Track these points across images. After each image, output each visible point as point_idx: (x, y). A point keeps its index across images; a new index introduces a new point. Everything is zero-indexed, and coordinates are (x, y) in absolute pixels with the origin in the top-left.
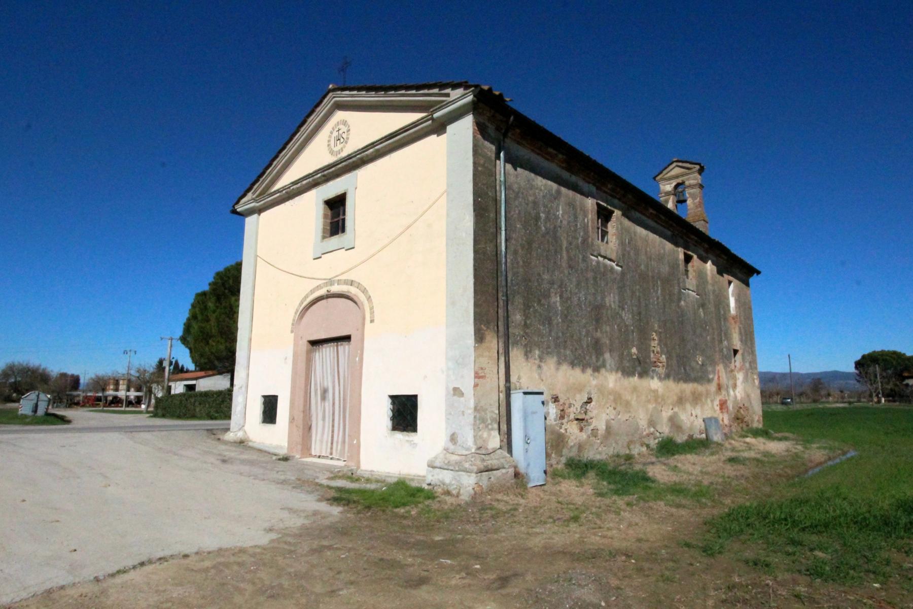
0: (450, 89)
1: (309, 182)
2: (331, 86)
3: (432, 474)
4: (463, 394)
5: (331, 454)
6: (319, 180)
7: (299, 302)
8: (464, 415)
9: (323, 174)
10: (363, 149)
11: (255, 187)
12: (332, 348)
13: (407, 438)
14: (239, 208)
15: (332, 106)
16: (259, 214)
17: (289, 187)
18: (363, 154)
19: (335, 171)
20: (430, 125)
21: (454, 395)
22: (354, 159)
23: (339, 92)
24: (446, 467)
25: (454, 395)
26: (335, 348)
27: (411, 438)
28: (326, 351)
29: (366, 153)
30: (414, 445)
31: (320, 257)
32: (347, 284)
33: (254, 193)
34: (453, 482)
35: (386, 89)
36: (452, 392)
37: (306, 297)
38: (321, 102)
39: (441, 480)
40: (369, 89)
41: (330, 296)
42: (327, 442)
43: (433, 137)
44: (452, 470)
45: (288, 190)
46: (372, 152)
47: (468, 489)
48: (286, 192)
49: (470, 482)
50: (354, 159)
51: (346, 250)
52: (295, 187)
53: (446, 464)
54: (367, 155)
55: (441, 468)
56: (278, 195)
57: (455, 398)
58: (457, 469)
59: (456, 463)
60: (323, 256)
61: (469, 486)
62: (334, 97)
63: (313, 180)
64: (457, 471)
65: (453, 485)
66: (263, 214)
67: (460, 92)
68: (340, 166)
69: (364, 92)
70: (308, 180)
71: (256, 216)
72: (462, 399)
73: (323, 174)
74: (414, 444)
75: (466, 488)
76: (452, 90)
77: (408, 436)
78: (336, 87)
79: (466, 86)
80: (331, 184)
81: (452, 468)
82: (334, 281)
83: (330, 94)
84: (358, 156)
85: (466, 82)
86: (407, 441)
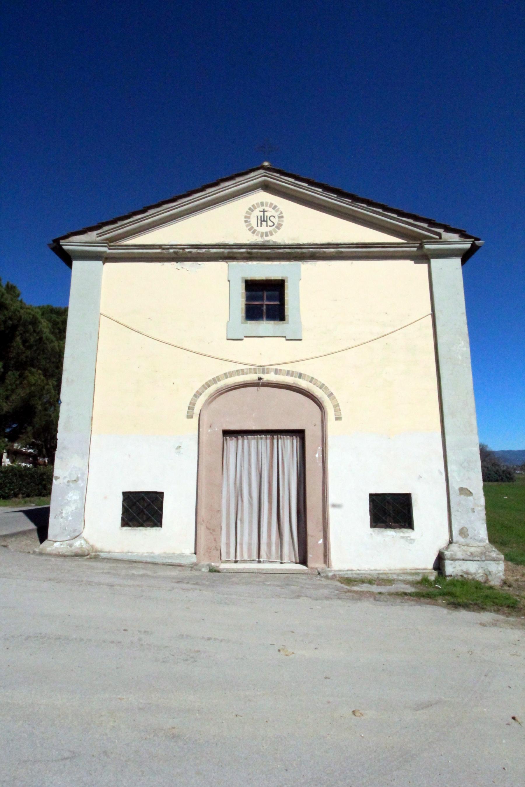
0: (443, 230)
1: (223, 253)
2: (266, 164)
3: (454, 566)
4: (472, 493)
5: (259, 556)
6: (238, 255)
7: (204, 383)
8: (474, 512)
9: (249, 250)
10: (321, 245)
11: (106, 228)
12: (263, 441)
13: (402, 535)
14: (68, 245)
15: (260, 182)
16: (104, 264)
17: (184, 249)
18: (318, 250)
19: (269, 253)
20: (413, 251)
21: (461, 494)
22: (304, 250)
23: (278, 175)
24: (471, 558)
25: (461, 494)
26: (268, 441)
27: (406, 535)
28: (287, 442)
29: (324, 250)
30: (412, 541)
31: (242, 340)
32: (292, 376)
33: (99, 235)
34: (479, 571)
35: (355, 199)
36: (458, 492)
37: (322, 387)
38: (247, 173)
39: (465, 570)
40: (326, 188)
41: (259, 384)
42: (250, 545)
43: (411, 263)
44: (478, 560)
45: (181, 250)
46: (333, 252)
47: (499, 574)
48: (175, 253)
49: (500, 569)
50: (304, 250)
51: (287, 340)
52: (194, 251)
53: (470, 556)
54: (324, 252)
55: (463, 560)
56: (159, 251)
57: (462, 496)
58: (484, 559)
59: (481, 553)
60: (245, 339)
61: (499, 573)
62: (265, 176)
63: (229, 253)
64: (484, 561)
65: (479, 573)
66: (107, 264)
67: (455, 237)
68: (276, 250)
69: (320, 190)
70: (222, 250)
71: (101, 263)
72: (471, 498)
73: (249, 250)
74: (411, 539)
75: (496, 574)
76: (445, 231)
77: (403, 532)
78: (272, 167)
79: (463, 235)
80: (254, 264)
81: (479, 559)
82: (268, 369)
83: (261, 171)
84: (311, 250)
85: (465, 231)
86: (402, 537)
